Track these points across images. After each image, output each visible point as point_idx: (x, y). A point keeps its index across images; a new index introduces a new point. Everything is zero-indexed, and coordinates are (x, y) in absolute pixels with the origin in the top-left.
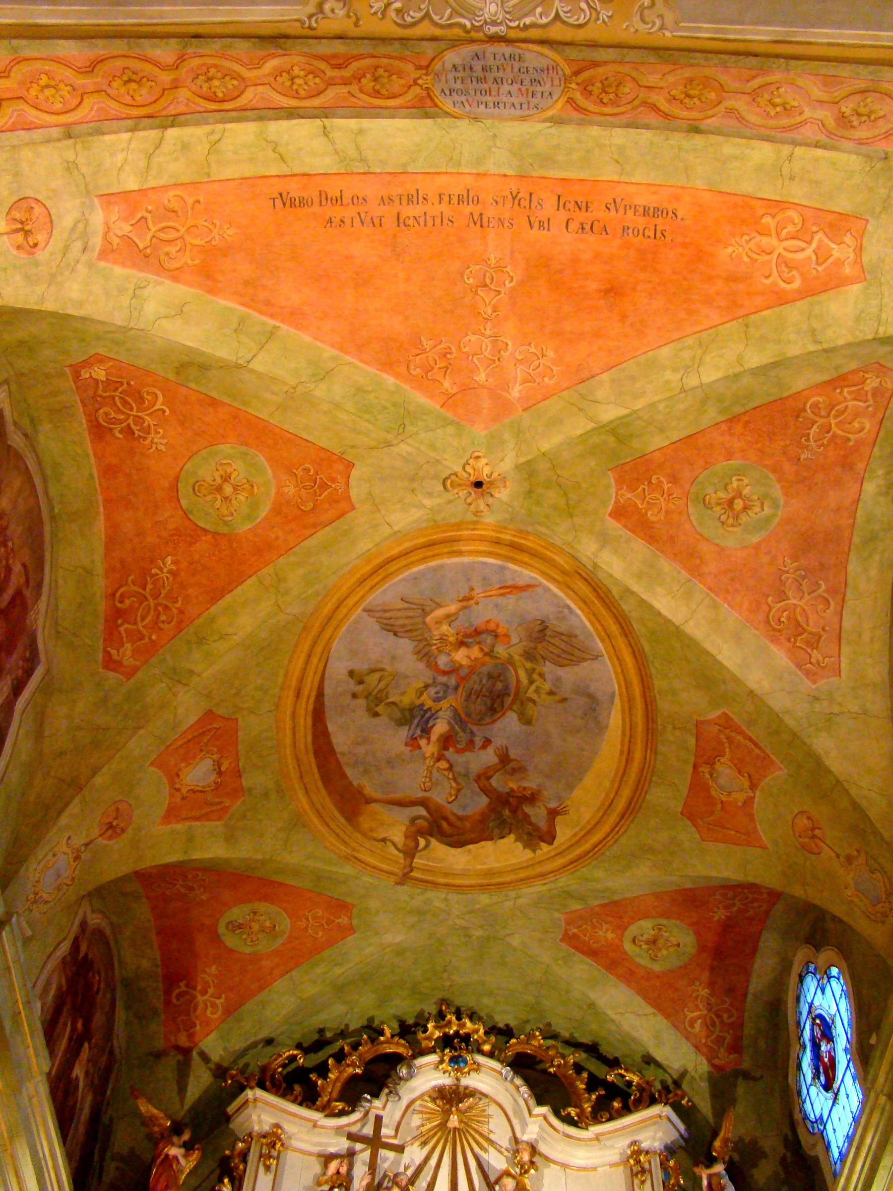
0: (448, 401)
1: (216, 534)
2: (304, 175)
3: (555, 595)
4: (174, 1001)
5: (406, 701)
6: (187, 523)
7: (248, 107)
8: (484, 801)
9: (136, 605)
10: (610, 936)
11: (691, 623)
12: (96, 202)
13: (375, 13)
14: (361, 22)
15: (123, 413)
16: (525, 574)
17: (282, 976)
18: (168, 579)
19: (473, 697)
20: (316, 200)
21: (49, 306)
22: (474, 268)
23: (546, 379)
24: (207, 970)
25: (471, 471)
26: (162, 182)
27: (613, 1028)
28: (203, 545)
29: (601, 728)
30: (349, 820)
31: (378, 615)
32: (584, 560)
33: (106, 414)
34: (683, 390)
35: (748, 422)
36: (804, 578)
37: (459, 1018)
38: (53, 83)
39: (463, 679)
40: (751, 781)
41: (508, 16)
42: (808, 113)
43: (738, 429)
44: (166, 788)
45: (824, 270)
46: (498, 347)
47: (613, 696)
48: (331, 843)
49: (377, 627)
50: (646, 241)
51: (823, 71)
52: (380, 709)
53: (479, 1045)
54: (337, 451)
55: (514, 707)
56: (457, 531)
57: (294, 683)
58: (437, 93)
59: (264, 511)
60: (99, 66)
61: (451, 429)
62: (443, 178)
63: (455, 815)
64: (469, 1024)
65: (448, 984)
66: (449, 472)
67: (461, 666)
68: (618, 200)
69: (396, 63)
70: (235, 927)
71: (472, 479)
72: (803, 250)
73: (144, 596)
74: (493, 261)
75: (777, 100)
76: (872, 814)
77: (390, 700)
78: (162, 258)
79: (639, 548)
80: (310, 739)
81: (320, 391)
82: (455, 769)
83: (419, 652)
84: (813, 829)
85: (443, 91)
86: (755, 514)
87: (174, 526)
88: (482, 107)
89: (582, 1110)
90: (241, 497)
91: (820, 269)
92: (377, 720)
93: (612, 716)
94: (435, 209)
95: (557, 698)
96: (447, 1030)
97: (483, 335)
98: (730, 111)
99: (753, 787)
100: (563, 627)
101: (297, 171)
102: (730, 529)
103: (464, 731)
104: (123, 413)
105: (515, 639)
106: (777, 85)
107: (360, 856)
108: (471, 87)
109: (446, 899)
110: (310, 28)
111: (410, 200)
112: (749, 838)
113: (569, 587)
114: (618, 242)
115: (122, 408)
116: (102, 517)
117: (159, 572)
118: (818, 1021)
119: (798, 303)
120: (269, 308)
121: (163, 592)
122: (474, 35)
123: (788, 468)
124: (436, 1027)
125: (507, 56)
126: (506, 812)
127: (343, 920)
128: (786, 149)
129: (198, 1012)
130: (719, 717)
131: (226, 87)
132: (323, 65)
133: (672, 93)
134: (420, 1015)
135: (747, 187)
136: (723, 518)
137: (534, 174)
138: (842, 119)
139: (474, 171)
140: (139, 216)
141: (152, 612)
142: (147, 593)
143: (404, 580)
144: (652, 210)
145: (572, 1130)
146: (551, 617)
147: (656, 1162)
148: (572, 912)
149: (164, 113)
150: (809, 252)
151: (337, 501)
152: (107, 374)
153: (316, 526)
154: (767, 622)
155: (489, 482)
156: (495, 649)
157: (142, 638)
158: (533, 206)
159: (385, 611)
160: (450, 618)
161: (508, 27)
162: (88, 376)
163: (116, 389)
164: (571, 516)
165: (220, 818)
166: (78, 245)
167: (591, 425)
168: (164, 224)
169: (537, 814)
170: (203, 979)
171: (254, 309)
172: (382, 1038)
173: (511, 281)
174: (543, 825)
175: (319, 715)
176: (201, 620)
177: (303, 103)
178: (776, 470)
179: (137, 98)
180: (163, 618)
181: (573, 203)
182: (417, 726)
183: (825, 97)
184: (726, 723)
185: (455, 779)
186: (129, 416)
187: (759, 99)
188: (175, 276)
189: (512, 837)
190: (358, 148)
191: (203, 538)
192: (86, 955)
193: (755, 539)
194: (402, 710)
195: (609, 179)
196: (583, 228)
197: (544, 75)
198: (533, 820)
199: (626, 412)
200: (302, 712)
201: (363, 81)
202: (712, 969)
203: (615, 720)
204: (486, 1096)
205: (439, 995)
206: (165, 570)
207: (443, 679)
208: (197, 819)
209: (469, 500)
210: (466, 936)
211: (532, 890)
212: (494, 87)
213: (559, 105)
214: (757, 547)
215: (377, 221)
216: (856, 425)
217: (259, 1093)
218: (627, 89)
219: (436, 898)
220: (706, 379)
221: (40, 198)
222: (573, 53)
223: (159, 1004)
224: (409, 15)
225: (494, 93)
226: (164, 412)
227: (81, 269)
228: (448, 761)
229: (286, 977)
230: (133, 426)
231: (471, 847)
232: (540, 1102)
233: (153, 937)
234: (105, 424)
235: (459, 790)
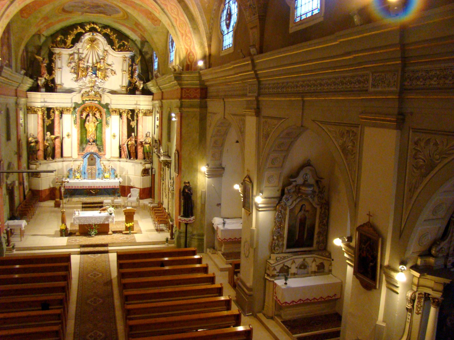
89: (116, 47)
145: (114, 51)
147: (127, 59)
204: (99, 39)
217: (57, 49)
232: (109, 44)
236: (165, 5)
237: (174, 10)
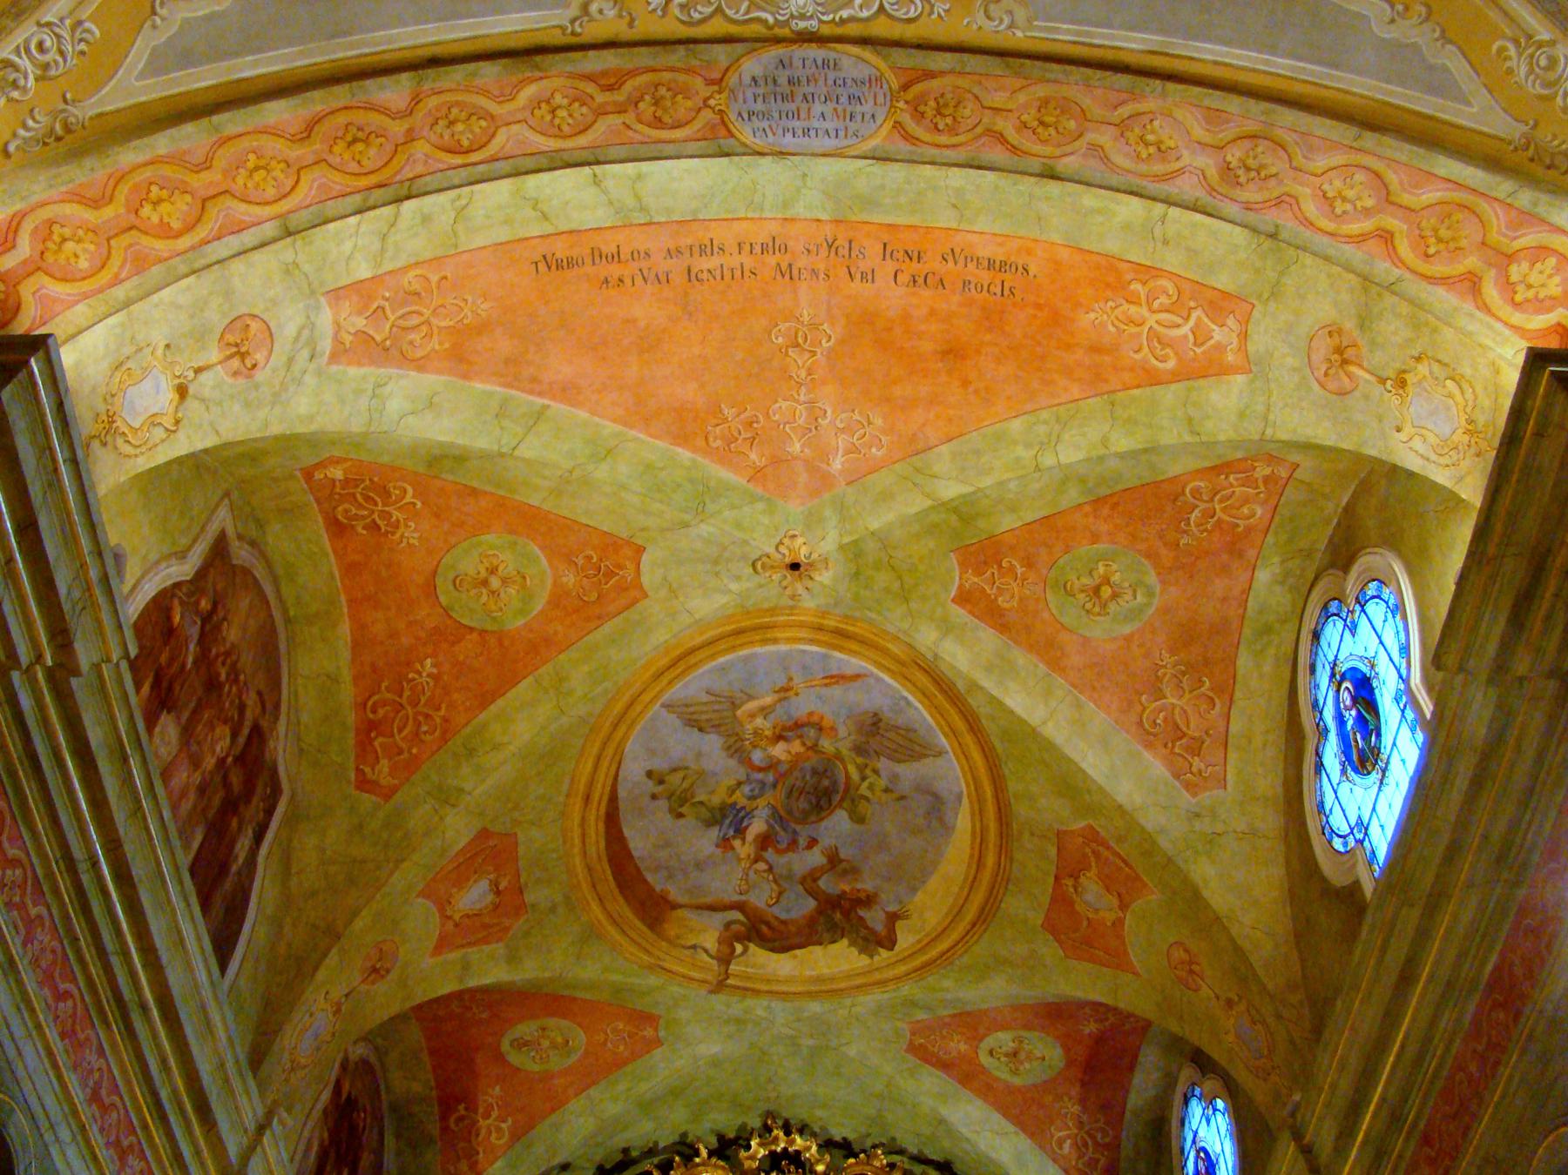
0: (757, 475)
1: (483, 633)
2: (571, 232)
3: (889, 686)
4: (452, 1126)
5: (716, 800)
6: (449, 622)
7: (500, 155)
8: (812, 904)
9: (392, 715)
10: (963, 1047)
11: (1050, 724)
12: (323, 300)
13: (654, 10)
14: (636, 23)
16: (853, 663)
17: (576, 1095)
19: (795, 794)
20: (588, 261)
21: (276, 429)
22: (783, 326)
23: (874, 450)
24: (490, 1090)
25: (786, 552)
26: (399, 264)
27: (968, 1147)
28: (467, 648)
29: (948, 829)
30: (651, 927)
31: (679, 710)
32: (923, 650)
33: (346, 511)
34: (1037, 468)
35: (1117, 504)
36: (1184, 673)
37: (788, 1133)
38: (262, 163)
39: (783, 775)
40: (1121, 901)
41: (820, 9)
42: (1187, 158)
43: (1106, 511)
44: (436, 918)
45: (1204, 353)
46: (815, 414)
47: (959, 798)
48: (632, 954)
49: (678, 723)
50: (992, 298)
51: (1207, 102)
52: (683, 810)
53: (812, 1165)
54: (624, 536)
55: (845, 805)
56: (772, 616)
57: (582, 788)
58: (733, 117)
59: (539, 605)
60: (316, 128)
61: (760, 506)
62: (744, 225)
63: (777, 918)
64: (799, 1140)
65: (773, 1095)
66: (759, 553)
67: (779, 762)
68: (957, 251)
69: (681, 77)
70: (520, 1044)
71: (788, 560)
72: (1178, 326)
73: (401, 705)
74: (806, 319)
75: (1150, 138)
76: (1256, 960)
77: (697, 799)
78: (405, 347)
79: (988, 638)
80: (602, 844)
81: (601, 472)
82: (775, 871)
83: (729, 748)
84: (1191, 963)
85: (740, 114)
86: (1127, 601)
88: (789, 136)
90: (512, 591)
91: (1199, 351)
92: (682, 821)
93: (960, 816)
94: (733, 260)
95: (895, 795)
96: (773, 1147)
97: (797, 401)
98: (1095, 150)
99: (1123, 907)
100: (900, 721)
101: (565, 228)
102: (1098, 618)
103: (784, 830)
105: (842, 732)
106: (1151, 116)
107: (666, 965)
108: (775, 107)
109: (769, 1007)
110: (573, 34)
111: (702, 252)
112: (1117, 960)
113: (906, 678)
114: (956, 299)
116: (347, 619)
117: (416, 676)
118: (1202, 1155)
119: (1173, 387)
120: (535, 386)
121: (423, 700)
122: (779, 32)
123: (1166, 556)
124: (761, 1145)
125: (820, 63)
126: (838, 916)
127: (649, 1032)
128: (1159, 208)
129: (480, 1138)
130: (1083, 829)
131: (472, 132)
132: (591, 89)
133: (1023, 118)
134: (743, 1127)
135: (1112, 246)
136: (1088, 606)
137: (854, 218)
138: (1227, 168)
139: (780, 216)
140: (375, 307)
141: (411, 722)
142: (404, 701)
143: (710, 671)
144: (998, 263)
146: (885, 708)
148: (918, 1022)
149: (398, 178)
150: (1185, 330)
151: (627, 589)
152: (345, 473)
153: (602, 619)
154: (1140, 723)
155: (808, 564)
156: (821, 742)
157: (401, 752)
158: (853, 255)
159: (686, 706)
160: (765, 711)
161: (821, 21)
162: (322, 476)
163: (357, 486)
164: (907, 600)
165: (499, 940)
166: (305, 353)
167: (929, 503)
168: (408, 309)
169: (874, 918)
170: (485, 1101)
171: (518, 389)
172: (697, 1160)
173: (828, 341)
174: (880, 928)
175: (612, 819)
176: (468, 730)
177: (569, 144)
178: (1150, 555)
179: (365, 162)
180: (425, 728)
181: (902, 253)
182: (730, 825)
183: (1208, 139)
184: (1091, 836)
185: (775, 881)
187: (1128, 134)
188: (420, 365)
189: (845, 942)
190: (636, 195)
191: (468, 637)
192: (350, 1093)
193: (1127, 629)
194: (711, 810)
195: (945, 226)
196: (915, 281)
197: (865, 89)
198: (870, 923)
199: (971, 489)
200: (593, 818)
201: (641, 105)
202: (1083, 1084)
203: (963, 822)
205: (763, 1107)
206: (424, 674)
207: (760, 776)
208: (470, 944)
209: (785, 583)
210: (794, 1044)
211: (868, 998)
212: (804, 106)
213: (884, 131)
214: (1128, 639)
215: (663, 279)
216: (1245, 510)
218: (968, 110)
219: (758, 1007)
220: (1064, 460)
221: (256, 311)
222: (903, 58)
223: (434, 1129)
224: (696, 10)
225: (803, 115)
226: (414, 504)
227: (310, 380)
228: (767, 862)
229: (584, 1094)
231: (798, 952)
233: (425, 1057)
234: (345, 521)
235: (780, 894)
236: (1279, 202)
237: (1350, 194)
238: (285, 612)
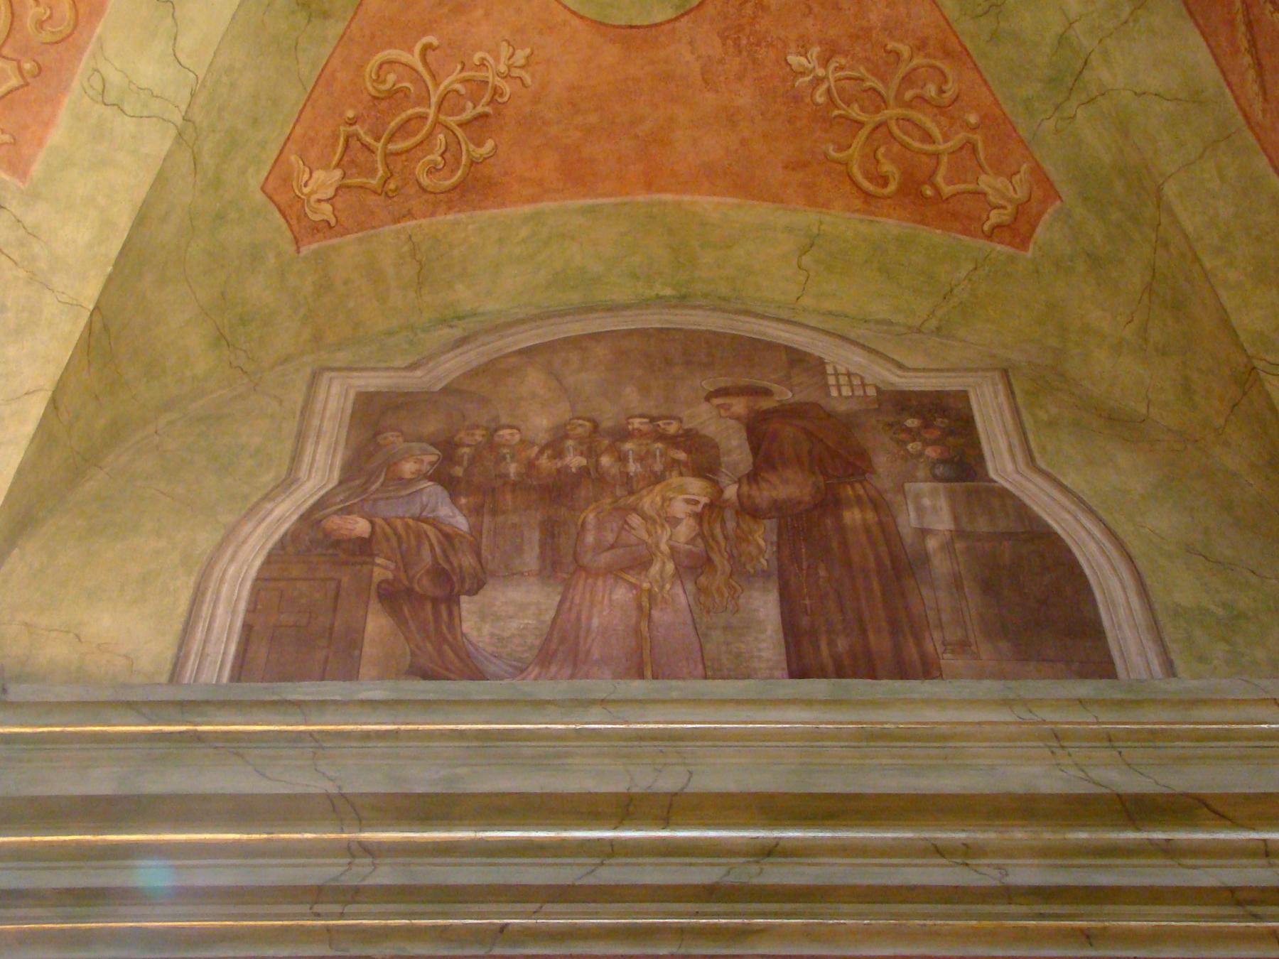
9: (896, 148)
15: (430, 135)
18: (841, 68)
33: (433, 170)
73: (877, 128)
78: (46, 36)
87: (717, 42)
104: (430, 135)
115: (419, 138)
116: (686, 198)
117: (823, 88)
141: (917, 116)
142: (870, 120)
152: (326, 168)
162: (327, 207)
180: (931, 90)
186: (437, 123)
206: (820, 72)
226: (427, 48)
230: (468, 114)
234: (460, 173)
238: (661, 302)
